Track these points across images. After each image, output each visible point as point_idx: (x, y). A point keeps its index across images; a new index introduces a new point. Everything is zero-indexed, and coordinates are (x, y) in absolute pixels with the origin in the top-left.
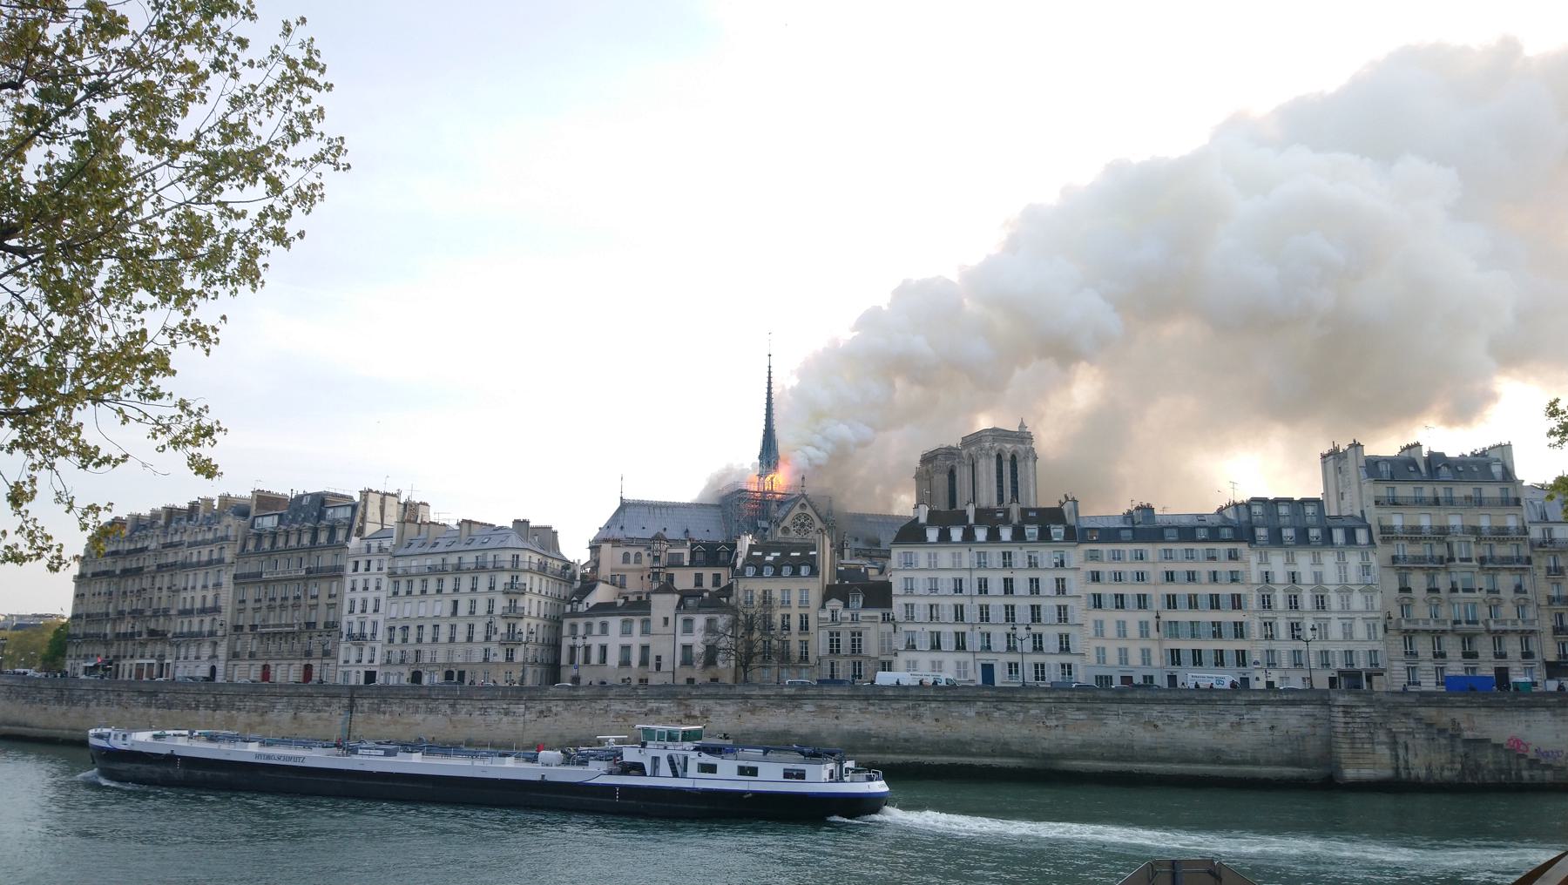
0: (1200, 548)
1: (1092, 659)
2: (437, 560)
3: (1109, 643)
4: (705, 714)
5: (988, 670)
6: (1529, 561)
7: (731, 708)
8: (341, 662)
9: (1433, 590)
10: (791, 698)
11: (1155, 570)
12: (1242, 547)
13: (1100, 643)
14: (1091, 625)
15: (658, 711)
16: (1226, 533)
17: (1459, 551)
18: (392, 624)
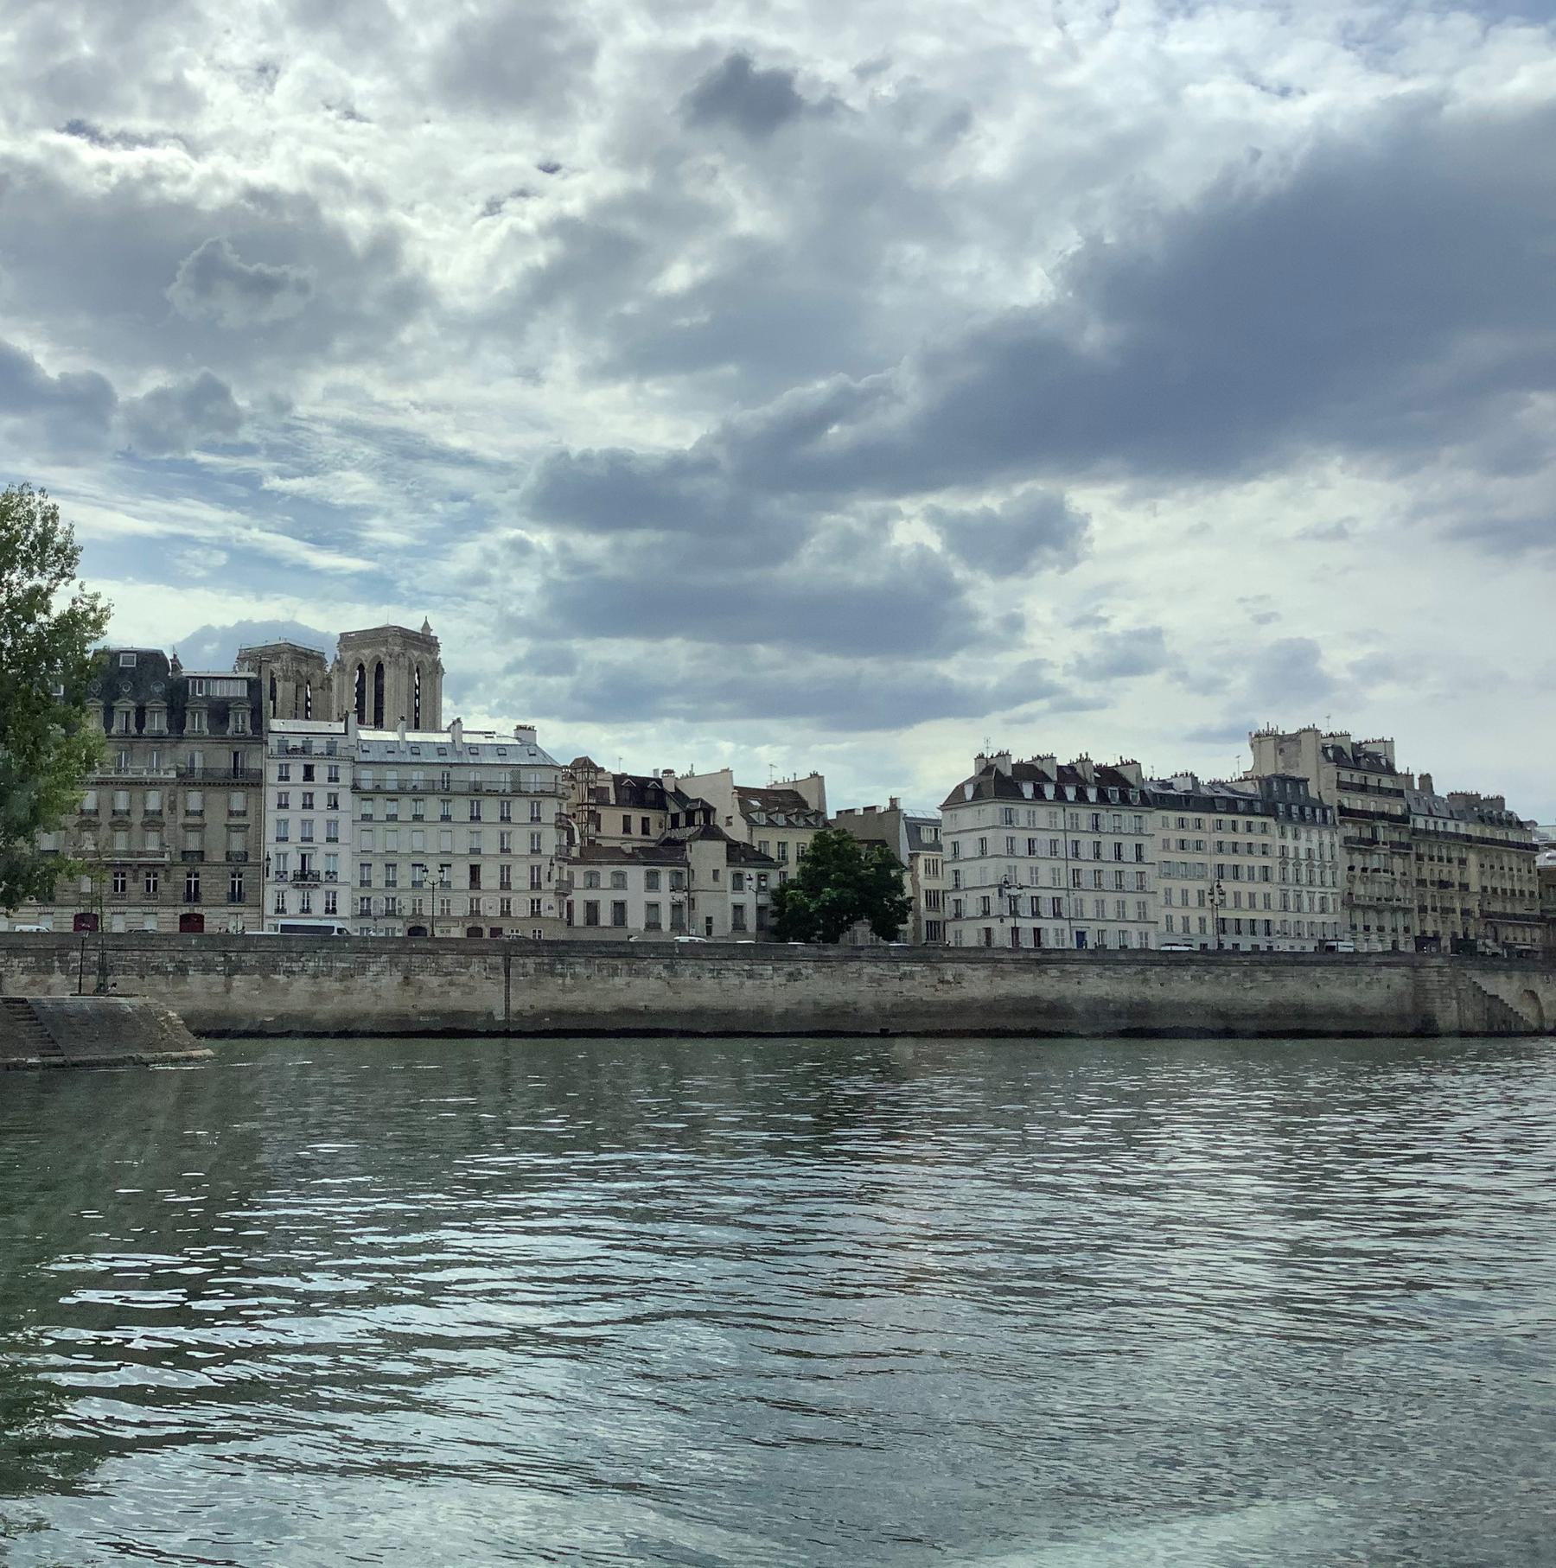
0: (1242, 820)
1: (1162, 927)
2: (436, 774)
3: (1171, 912)
4: (958, 979)
5: (1081, 936)
6: (1409, 847)
7: (982, 973)
8: (269, 909)
9: (1351, 868)
10: (1038, 962)
11: (1211, 838)
12: (1270, 821)
13: (1168, 911)
14: (1161, 892)
15: (911, 975)
16: (1258, 807)
17: (1382, 835)
18: (367, 859)
